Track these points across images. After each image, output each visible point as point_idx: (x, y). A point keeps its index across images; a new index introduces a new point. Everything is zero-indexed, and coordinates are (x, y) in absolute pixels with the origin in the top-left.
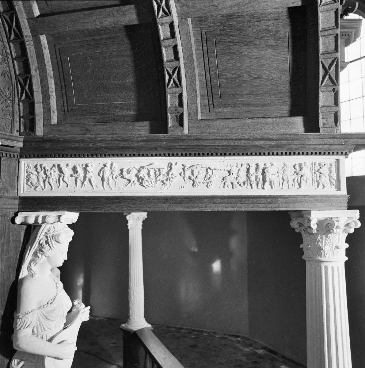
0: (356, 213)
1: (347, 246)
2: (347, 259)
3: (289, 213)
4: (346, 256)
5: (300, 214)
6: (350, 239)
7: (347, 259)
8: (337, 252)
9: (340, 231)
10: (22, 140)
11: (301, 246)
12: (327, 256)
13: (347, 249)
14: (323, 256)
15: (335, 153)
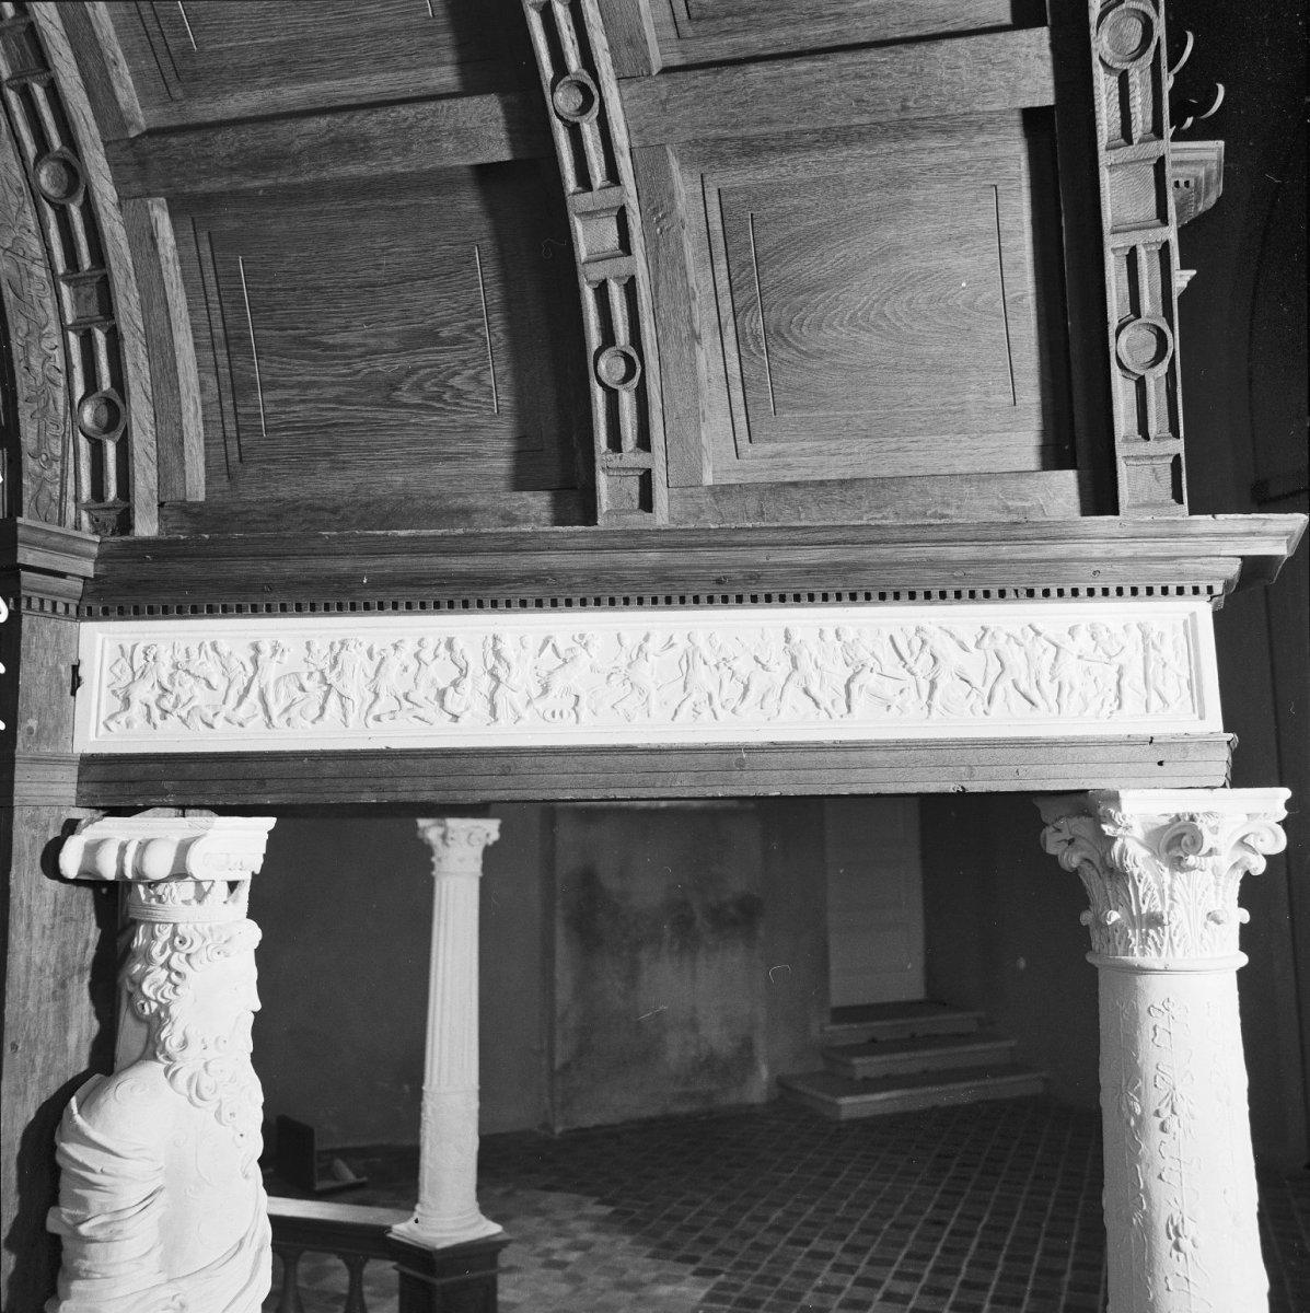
0: (1273, 801)
1: (1244, 916)
2: (1243, 960)
3: (1040, 804)
4: (1242, 949)
5: (1086, 806)
6: (1251, 891)
7: (1243, 960)
8: (1211, 940)
9: (1224, 860)
10: (95, 550)
11: (1086, 918)
12: (1179, 952)
13: (1243, 927)
14: (1164, 949)
15: (1188, 590)
